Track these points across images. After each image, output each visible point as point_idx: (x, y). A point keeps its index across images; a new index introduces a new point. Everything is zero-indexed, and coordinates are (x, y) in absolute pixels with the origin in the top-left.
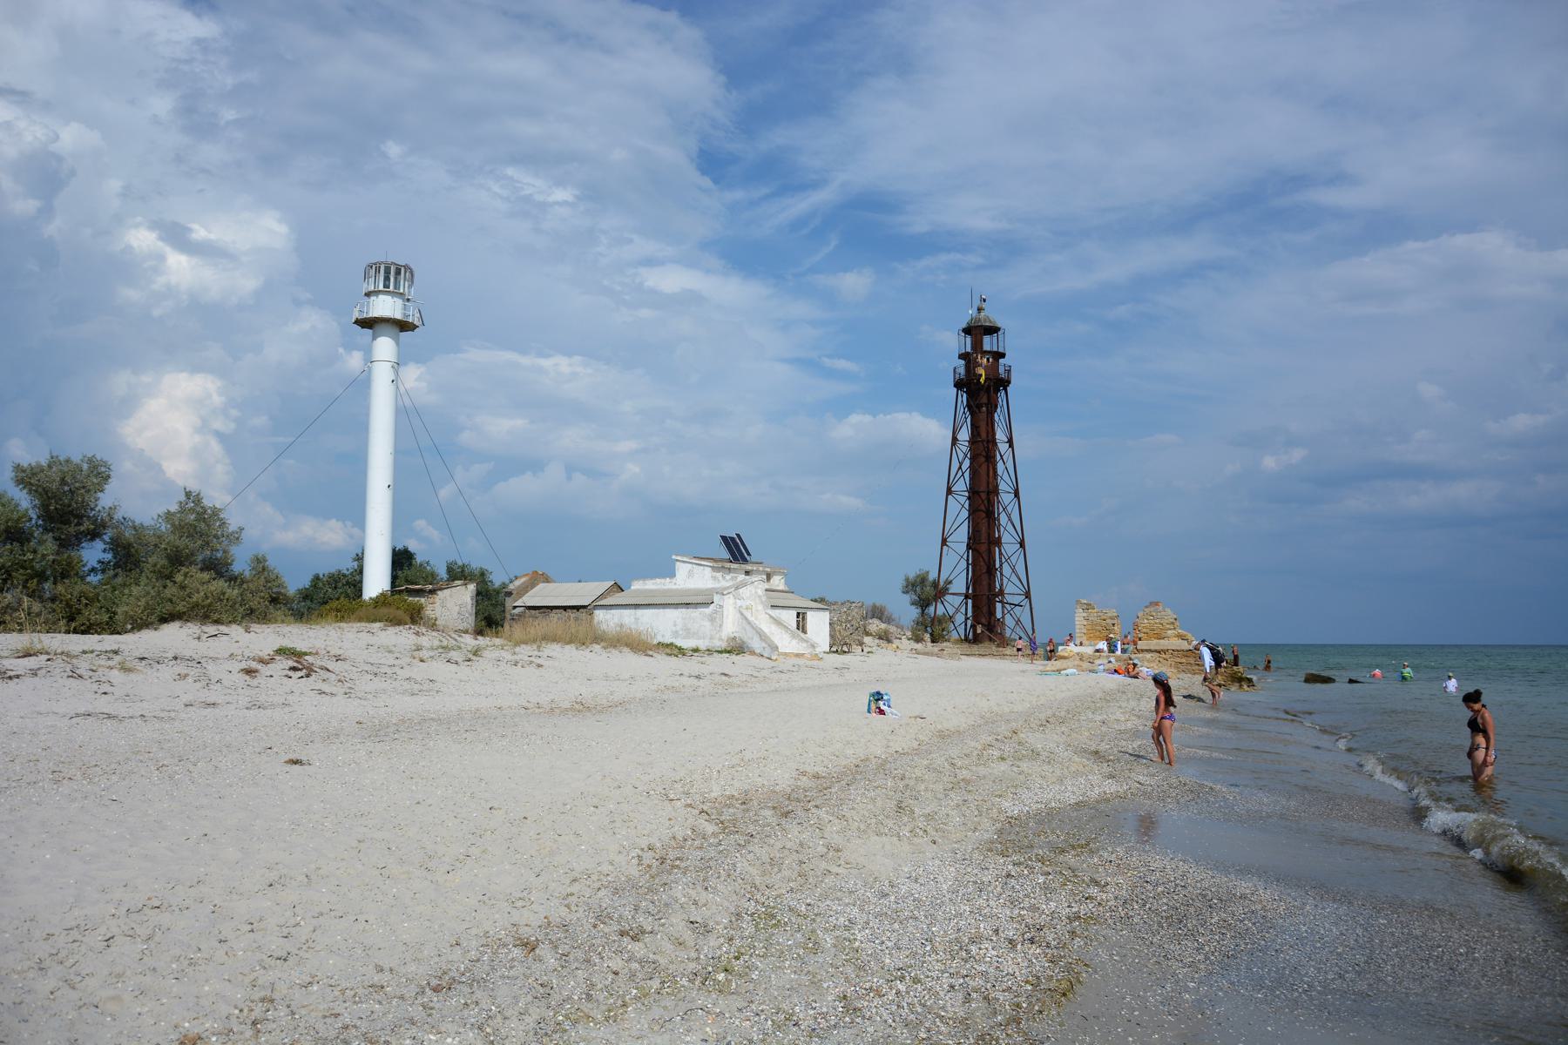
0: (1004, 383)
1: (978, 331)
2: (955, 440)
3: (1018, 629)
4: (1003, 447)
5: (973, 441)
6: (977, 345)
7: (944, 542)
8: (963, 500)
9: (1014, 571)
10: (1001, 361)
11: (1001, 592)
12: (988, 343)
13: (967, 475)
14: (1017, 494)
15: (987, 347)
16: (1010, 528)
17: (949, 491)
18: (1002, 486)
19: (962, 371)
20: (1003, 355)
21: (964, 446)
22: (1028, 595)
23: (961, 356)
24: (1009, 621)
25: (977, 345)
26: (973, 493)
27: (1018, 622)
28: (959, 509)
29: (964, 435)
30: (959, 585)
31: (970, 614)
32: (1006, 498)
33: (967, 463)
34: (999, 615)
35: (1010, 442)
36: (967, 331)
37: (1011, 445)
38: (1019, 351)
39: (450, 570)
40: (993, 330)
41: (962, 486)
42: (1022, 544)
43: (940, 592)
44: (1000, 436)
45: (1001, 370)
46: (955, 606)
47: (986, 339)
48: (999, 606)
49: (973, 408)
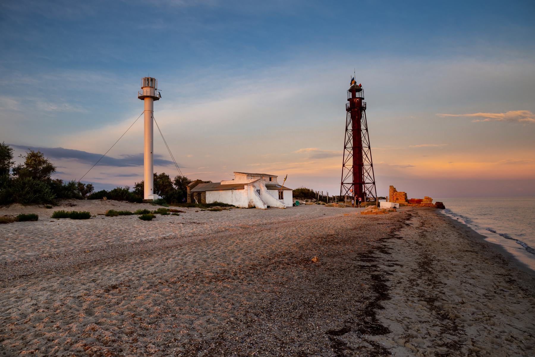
2: (347, 129)
4: (364, 132)
6: (354, 96)
8: (350, 150)
10: (363, 101)
12: (358, 95)
13: (352, 141)
15: (357, 96)
17: (345, 148)
19: (349, 105)
20: (363, 99)
21: (350, 132)
23: (348, 100)
25: (354, 96)
26: (354, 148)
29: (350, 127)
35: (367, 129)
36: (350, 91)
37: (367, 131)
38: (368, 96)
39: (161, 183)
41: (350, 145)
44: (363, 127)
45: (363, 104)
49: (353, 117)
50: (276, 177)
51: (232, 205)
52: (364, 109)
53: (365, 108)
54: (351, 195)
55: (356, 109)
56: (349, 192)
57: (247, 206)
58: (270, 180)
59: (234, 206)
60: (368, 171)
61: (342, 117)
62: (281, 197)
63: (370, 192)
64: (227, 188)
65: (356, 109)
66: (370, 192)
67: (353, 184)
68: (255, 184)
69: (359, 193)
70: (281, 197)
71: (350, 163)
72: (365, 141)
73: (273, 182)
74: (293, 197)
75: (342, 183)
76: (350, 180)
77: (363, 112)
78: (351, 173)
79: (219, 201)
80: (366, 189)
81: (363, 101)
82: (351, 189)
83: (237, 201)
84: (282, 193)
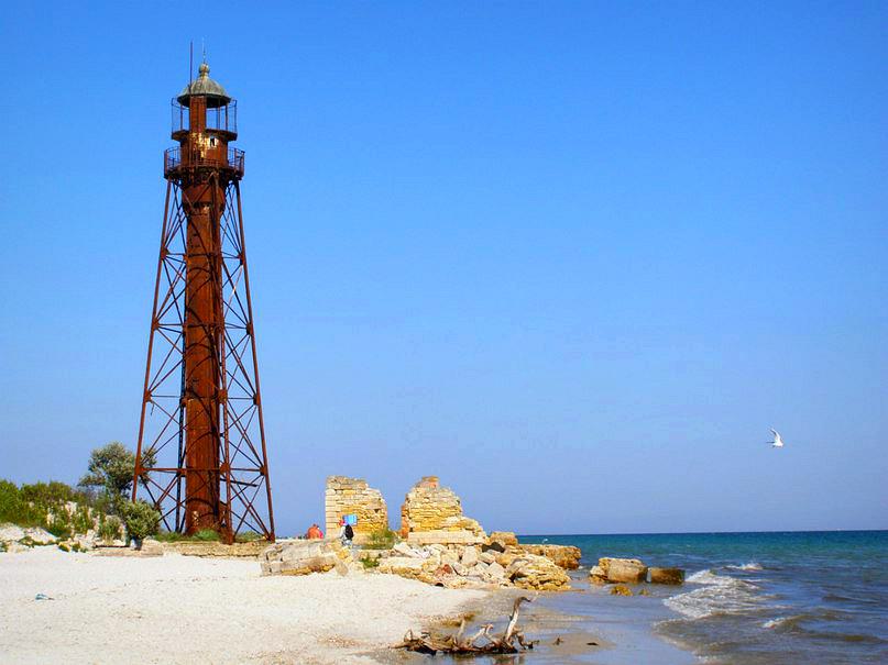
0: (232, 176)
1: (201, 103)
2: (164, 253)
3: (249, 518)
4: (231, 264)
5: (190, 254)
6: (197, 122)
7: (147, 396)
8: (174, 336)
9: (244, 435)
10: (230, 144)
11: (227, 464)
12: (212, 118)
13: (181, 302)
14: (250, 330)
15: (211, 124)
16: (239, 376)
17: (155, 325)
18: (229, 318)
19: (176, 155)
20: (233, 137)
21: (176, 264)
22: (264, 471)
23: (175, 136)
24: (237, 507)
25: (197, 122)
27: (249, 507)
28: (169, 350)
29: (177, 246)
30: (168, 457)
31: (183, 498)
32: (235, 335)
33: (181, 285)
34: (223, 498)
35: (242, 257)
37: (243, 262)
40: (218, 101)
41: (173, 317)
42: (256, 400)
43: (141, 469)
44: (228, 248)
45: (231, 156)
46: (162, 490)
47: (211, 113)
48: (223, 485)
53: (240, 174)
61: (150, 203)
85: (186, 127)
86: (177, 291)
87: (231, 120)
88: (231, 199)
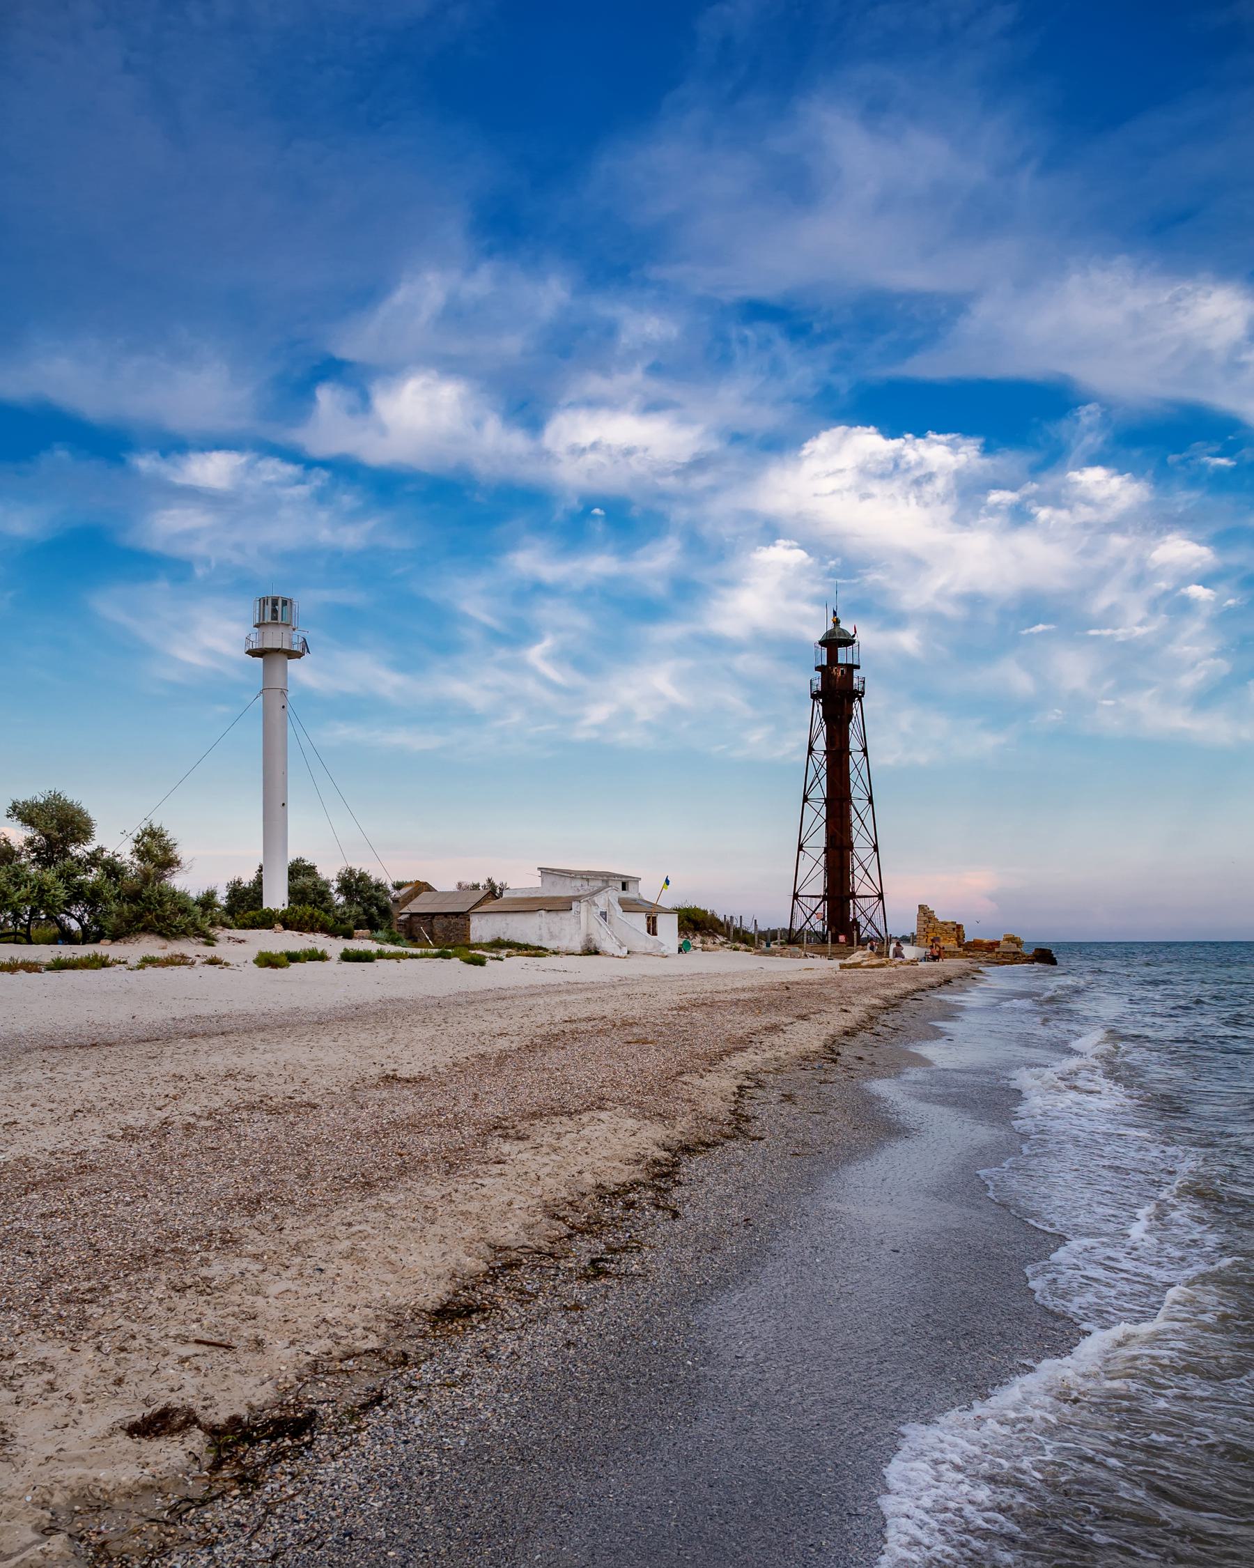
2: (811, 750)
6: (832, 657)
7: (800, 847)
8: (818, 806)
14: (871, 800)
17: (805, 799)
20: (858, 667)
21: (820, 757)
23: (817, 669)
25: (832, 657)
26: (828, 802)
28: (816, 815)
29: (820, 744)
33: (823, 771)
35: (865, 751)
37: (866, 754)
40: (849, 642)
41: (820, 792)
42: (876, 848)
44: (854, 744)
45: (855, 681)
47: (841, 650)
49: (826, 716)
50: (637, 880)
51: (540, 948)
52: (859, 695)
53: (863, 693)
54: (819, 927)
55: (837, 695)
56: (813, 921)
57: (579, 950)
58: (624, 888)
59: (546, 950)
60: (866, 865)
62: (652, 930)
63: (870, 921)
64: (534, 907)
65: (837, 695)
66: (870, 921)
67: (824, 898)
68: (595, 899)
69: (839, 919)
70: (652, 930)
71: (819, 840)
72: (859, 783)
73: (630, 894)
74: (680, 930)
75: (796, 896)
76: (816, 885)
77: (856, 704)
78: (820, 869)
79: (505, 938)
80: (858, 912)
81: (856, 673)
82: (820, 910)
83: (552, 936)
84: (654, 919)
85: (825, 663)
86: (820, 776)
87: (856, 656)
88: (856, 710)
